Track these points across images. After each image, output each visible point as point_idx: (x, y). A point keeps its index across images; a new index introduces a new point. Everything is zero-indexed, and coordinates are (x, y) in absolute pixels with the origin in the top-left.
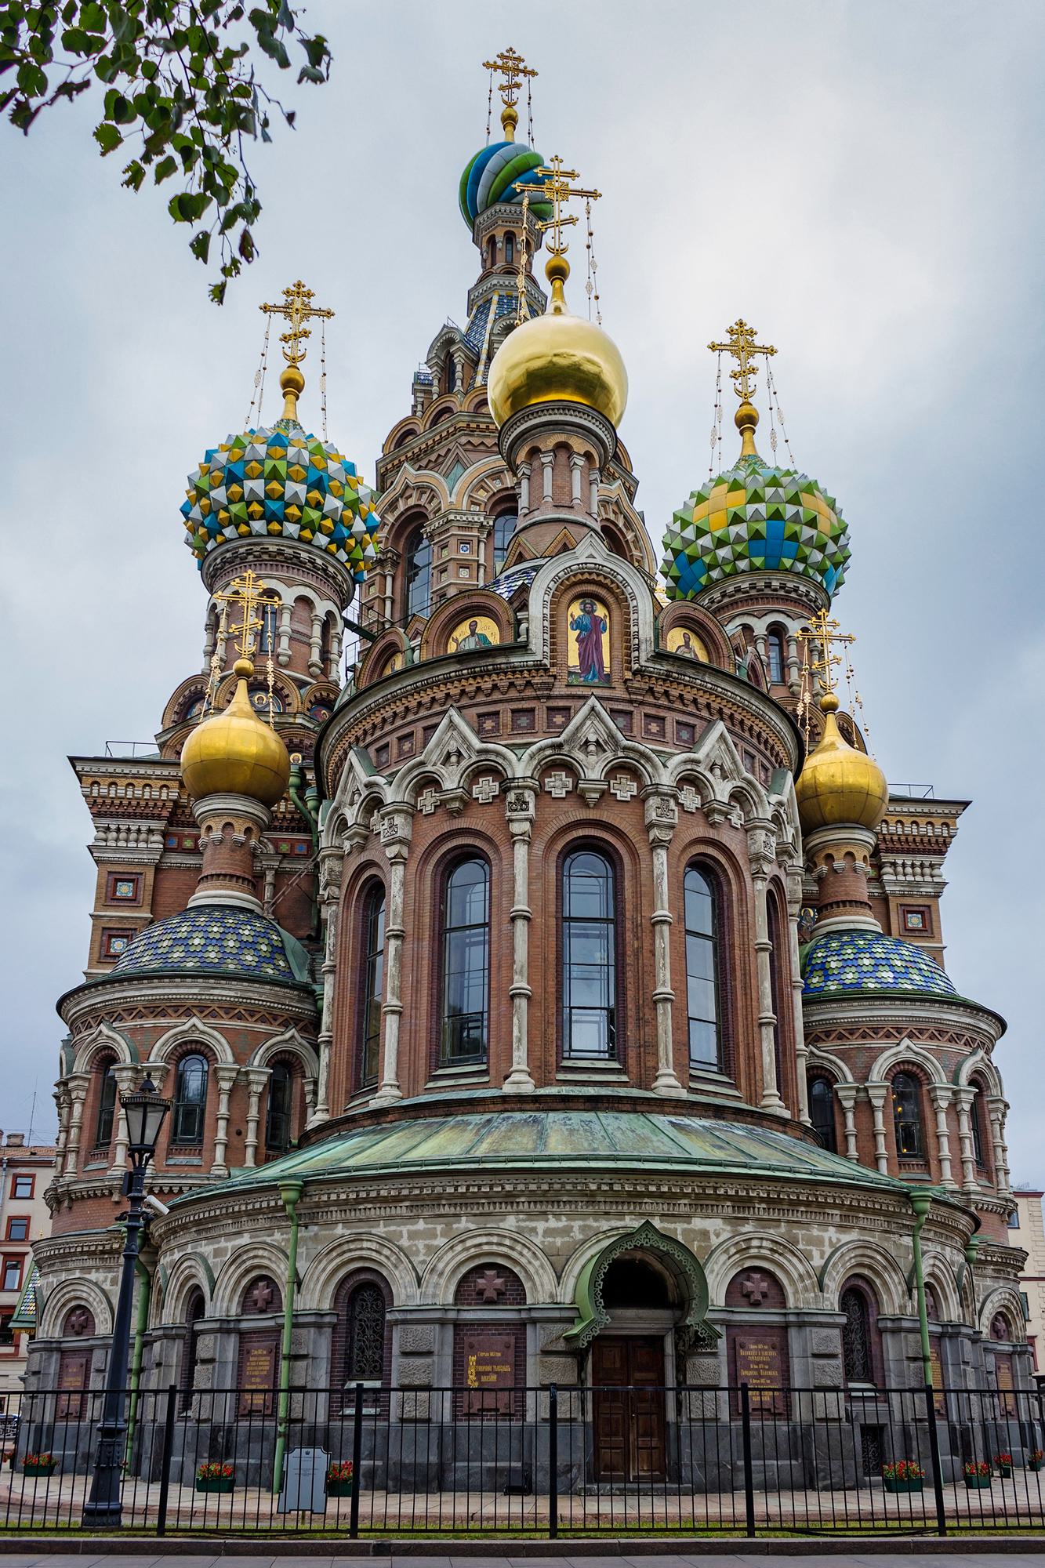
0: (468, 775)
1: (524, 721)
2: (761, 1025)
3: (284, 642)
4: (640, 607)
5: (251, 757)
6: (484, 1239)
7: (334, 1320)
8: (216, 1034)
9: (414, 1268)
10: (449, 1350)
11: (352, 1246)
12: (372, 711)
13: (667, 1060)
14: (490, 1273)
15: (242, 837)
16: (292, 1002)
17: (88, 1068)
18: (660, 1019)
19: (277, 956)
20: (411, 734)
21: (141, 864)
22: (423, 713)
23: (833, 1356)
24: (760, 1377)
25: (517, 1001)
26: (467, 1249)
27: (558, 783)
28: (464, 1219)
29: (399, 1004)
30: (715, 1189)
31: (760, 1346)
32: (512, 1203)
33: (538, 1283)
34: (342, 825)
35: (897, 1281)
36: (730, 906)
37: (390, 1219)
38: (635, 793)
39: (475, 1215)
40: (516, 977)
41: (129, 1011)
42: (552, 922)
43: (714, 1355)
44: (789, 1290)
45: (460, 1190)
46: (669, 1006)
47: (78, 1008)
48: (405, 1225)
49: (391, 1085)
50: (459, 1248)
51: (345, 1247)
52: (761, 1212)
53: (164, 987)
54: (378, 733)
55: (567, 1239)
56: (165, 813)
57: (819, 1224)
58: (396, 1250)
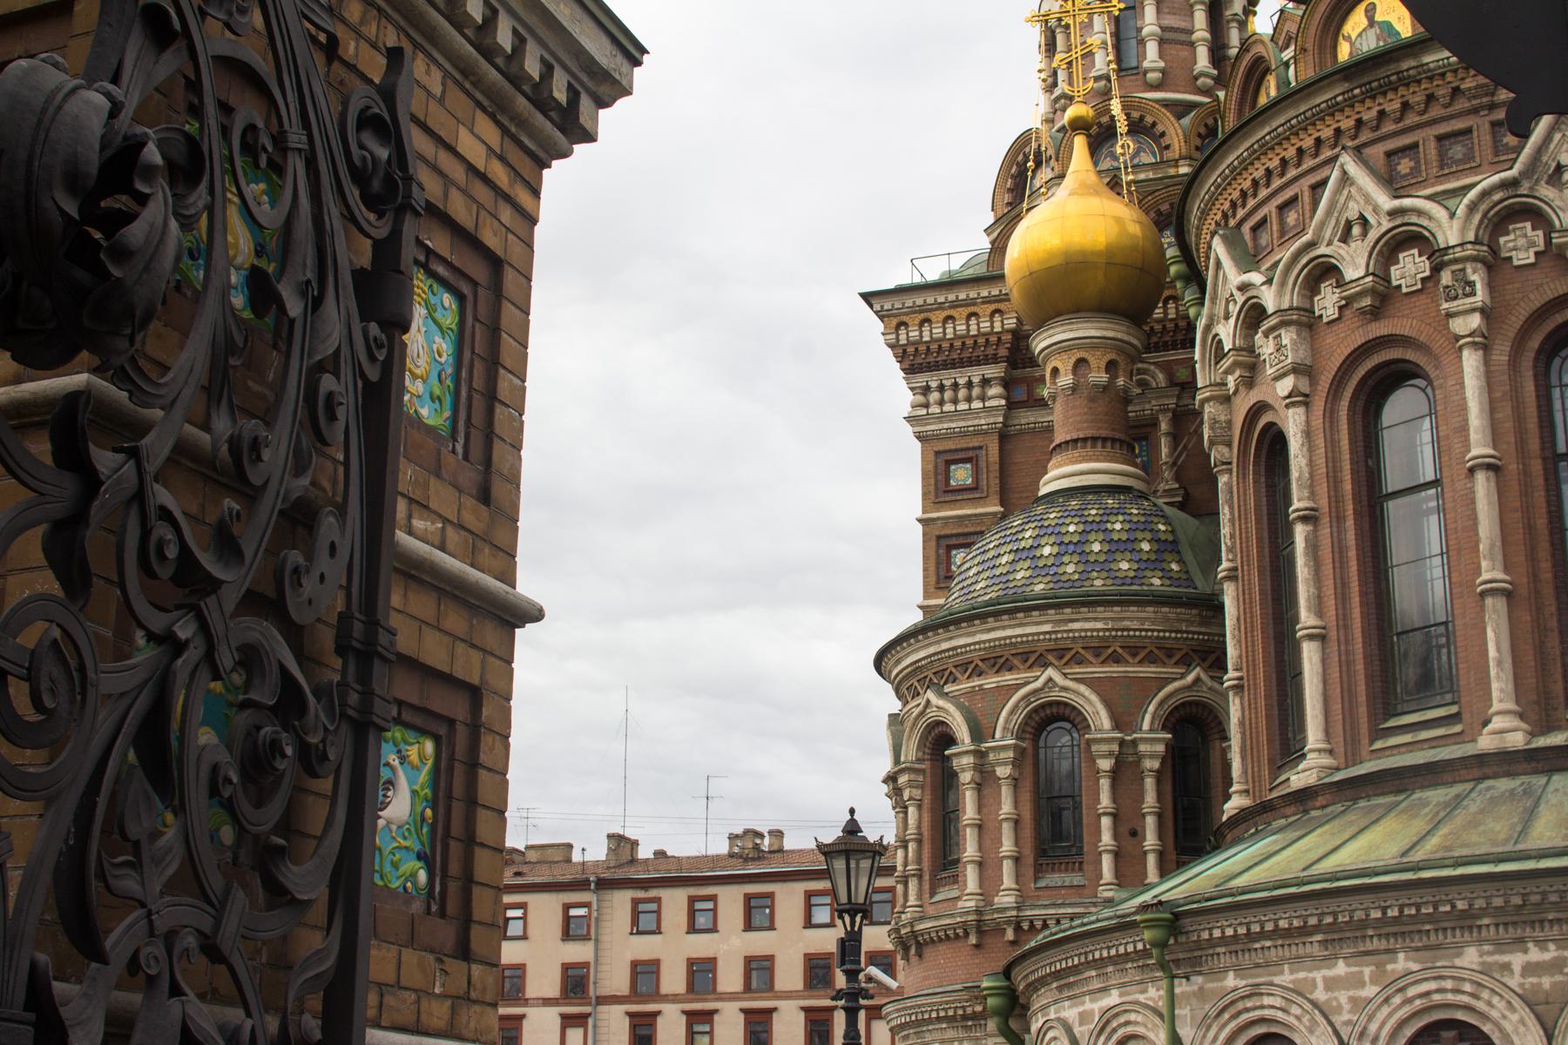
0: (1380, 251)
1: (1457, 151)
3: (1152, 49)
5: (1098, 254)
6: (1432, 985)
8: (1082, 688)
11: (1249, 1004)
12: (1236, 172)
14: (1448, 1035)
15: (1103, 377)
16: (1188, 625)
17: (920, 754)
19: (1167, 556)
20: (1293, 200)
21: (978, 433)
22: (1309, 163)
25: (1489, 601)
26: (1409, 1001)
27: (1521, 242)
28: (1401, 956)
29: (1319, 623)
34: (1220, 354)
37: (1297, 961)
39: (1417, 949)
40: (1484, 564)
41: (963, 666)
42: (1537, 466)
47: (899, 668)
48: (1319, 968)
49: (1319, 750)
50: (1397, 1000)
51: (1240, 1006)
53: (1004, 628)
54: (1251, 203)
55: (1559, 978)
56: (1003, 352)
58: (1308, 1006)
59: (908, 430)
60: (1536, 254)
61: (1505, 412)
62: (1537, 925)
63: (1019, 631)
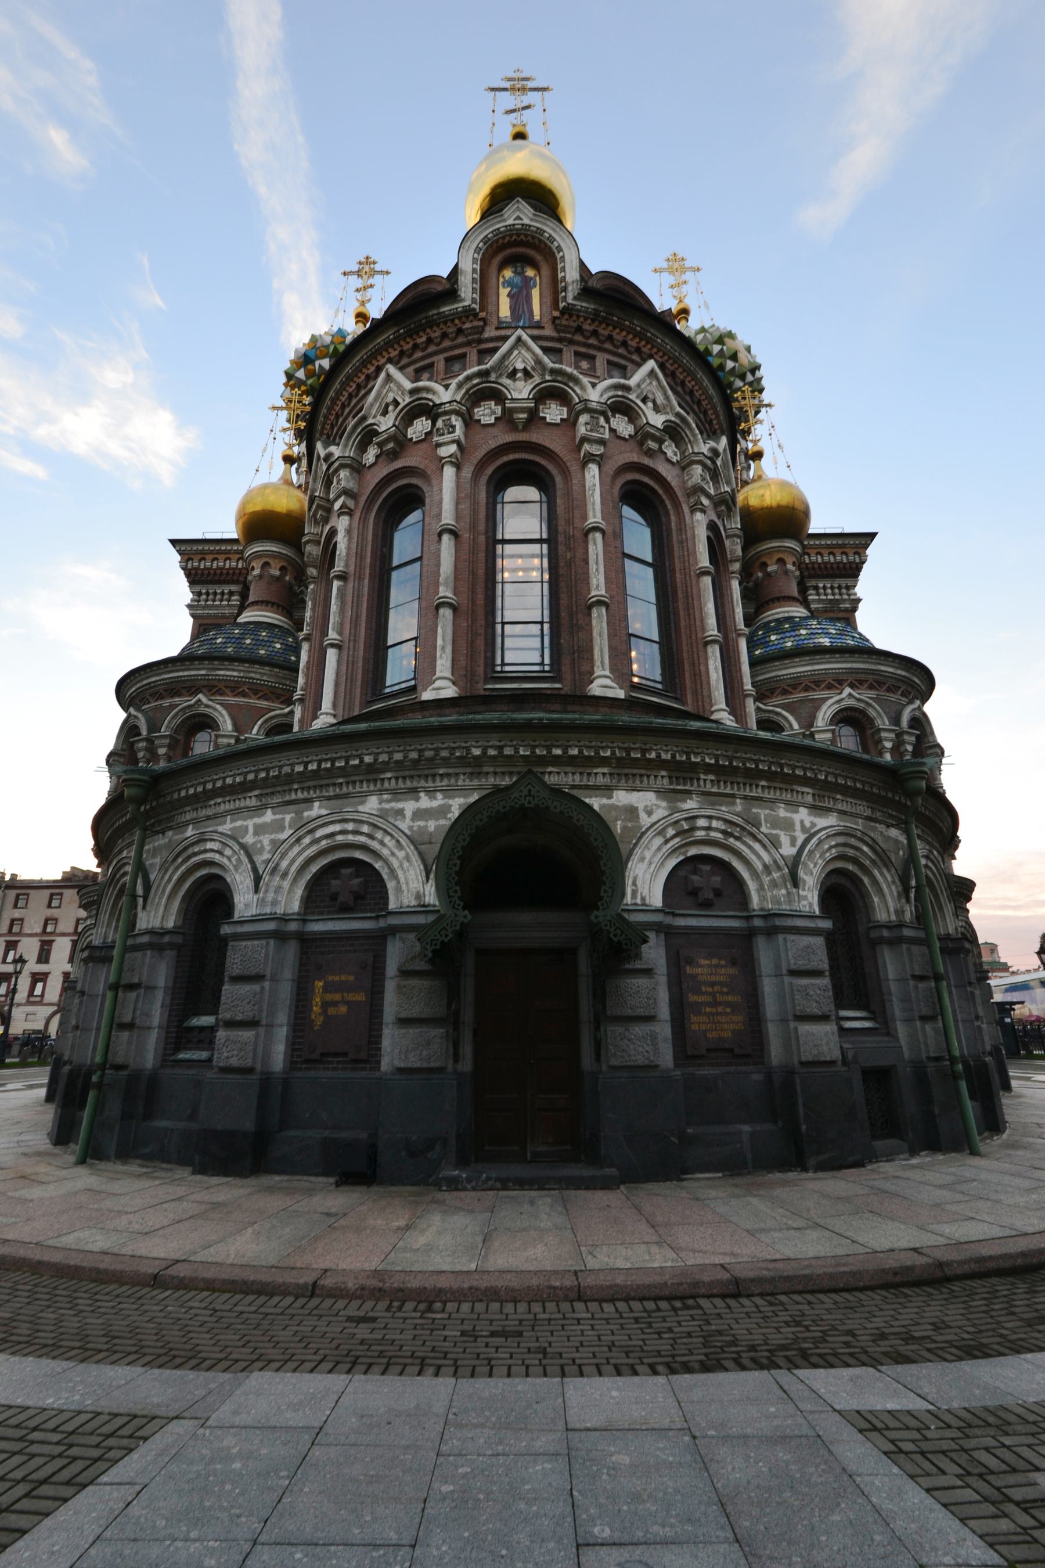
0: (402, 418)
2: (707, 644)
4: (566, 257)
6: (337, 828)
7: (178, 939)
9: (255, 869)
10: (288, 973)
11: (196, 849)
13: (602, 663)
14: (346, 871)
15: (278, 573)
18: (594, 622)
23: (816, 973)
24: (715, 1004)
25: (441, 611)
27: (487, 411)
28: (316, 804)
29: (338, 637)
30: (644, 751)
31: (715, 961)
32: (375, 780)
33: (402, 880)
35: (889, 879)
36: (669, 534)
37: (236, 813)
38: (565, 416)
39: (329, 798)
40: (441, 589)
42: (482, 539)
43: (648, 972)
44: (752, 886)
45: (310, 767)
46: (604, 610)
48: (252, 817)
49: (327, 714)
50: (307, 840)
51: (190, 851)
52: (709, 785)
53: (177, 671)
55: (442, 822)
57: (787, 803)
58: (236, 847)
59: (187, 611)
60: (496, 419)
61: (465, 506)
62: (430, 778)
63: (186, 673)
